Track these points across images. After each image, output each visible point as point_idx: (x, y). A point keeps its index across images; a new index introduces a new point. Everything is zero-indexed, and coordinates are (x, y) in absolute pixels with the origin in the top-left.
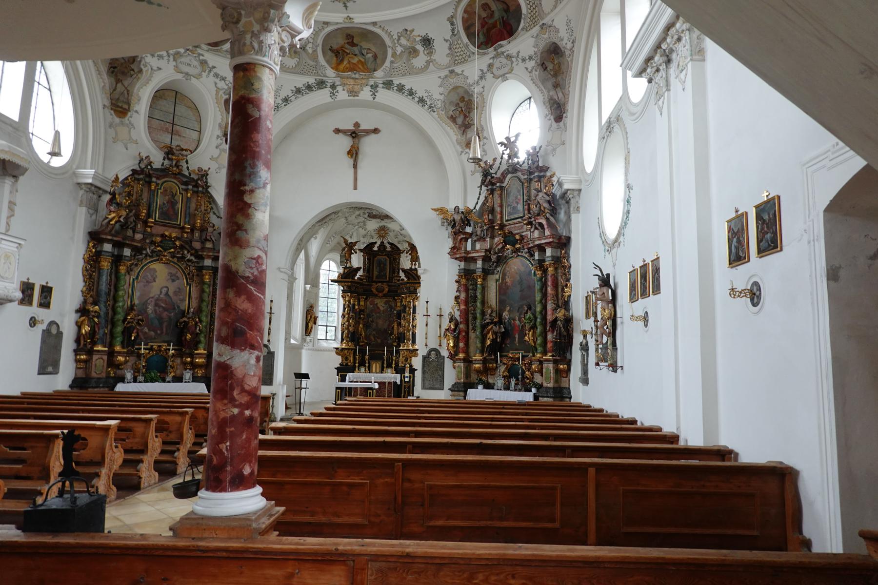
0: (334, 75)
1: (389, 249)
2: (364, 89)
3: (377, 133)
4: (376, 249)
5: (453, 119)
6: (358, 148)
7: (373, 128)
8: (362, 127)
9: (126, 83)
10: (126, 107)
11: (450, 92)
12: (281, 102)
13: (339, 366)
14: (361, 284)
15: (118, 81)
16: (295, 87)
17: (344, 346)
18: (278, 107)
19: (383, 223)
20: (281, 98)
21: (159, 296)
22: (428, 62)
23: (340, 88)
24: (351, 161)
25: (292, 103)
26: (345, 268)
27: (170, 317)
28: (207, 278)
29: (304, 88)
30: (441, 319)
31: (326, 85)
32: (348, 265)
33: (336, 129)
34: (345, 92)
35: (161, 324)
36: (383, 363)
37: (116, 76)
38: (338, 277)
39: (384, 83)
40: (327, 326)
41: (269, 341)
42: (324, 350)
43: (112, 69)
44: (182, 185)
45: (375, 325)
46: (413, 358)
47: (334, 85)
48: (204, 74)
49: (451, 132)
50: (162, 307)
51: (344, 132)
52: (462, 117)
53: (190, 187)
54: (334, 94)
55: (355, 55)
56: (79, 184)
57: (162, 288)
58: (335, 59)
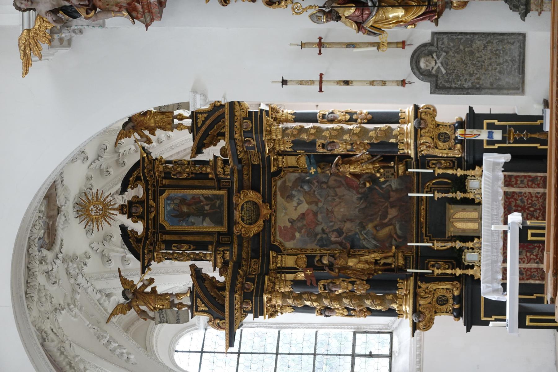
1: (139, 191)
4: (139, 227)
13: (461, 320)
14: (238, 265)
17: (408, 308)
19: (69, 209)
26: (194, 309)
30: (332, 44)
32: (187, 301)
36: (454, 201)
38: (219, 327)
40: (354, 356)
42: (420, 362)
45: (348, 225)
46: (439, 119)
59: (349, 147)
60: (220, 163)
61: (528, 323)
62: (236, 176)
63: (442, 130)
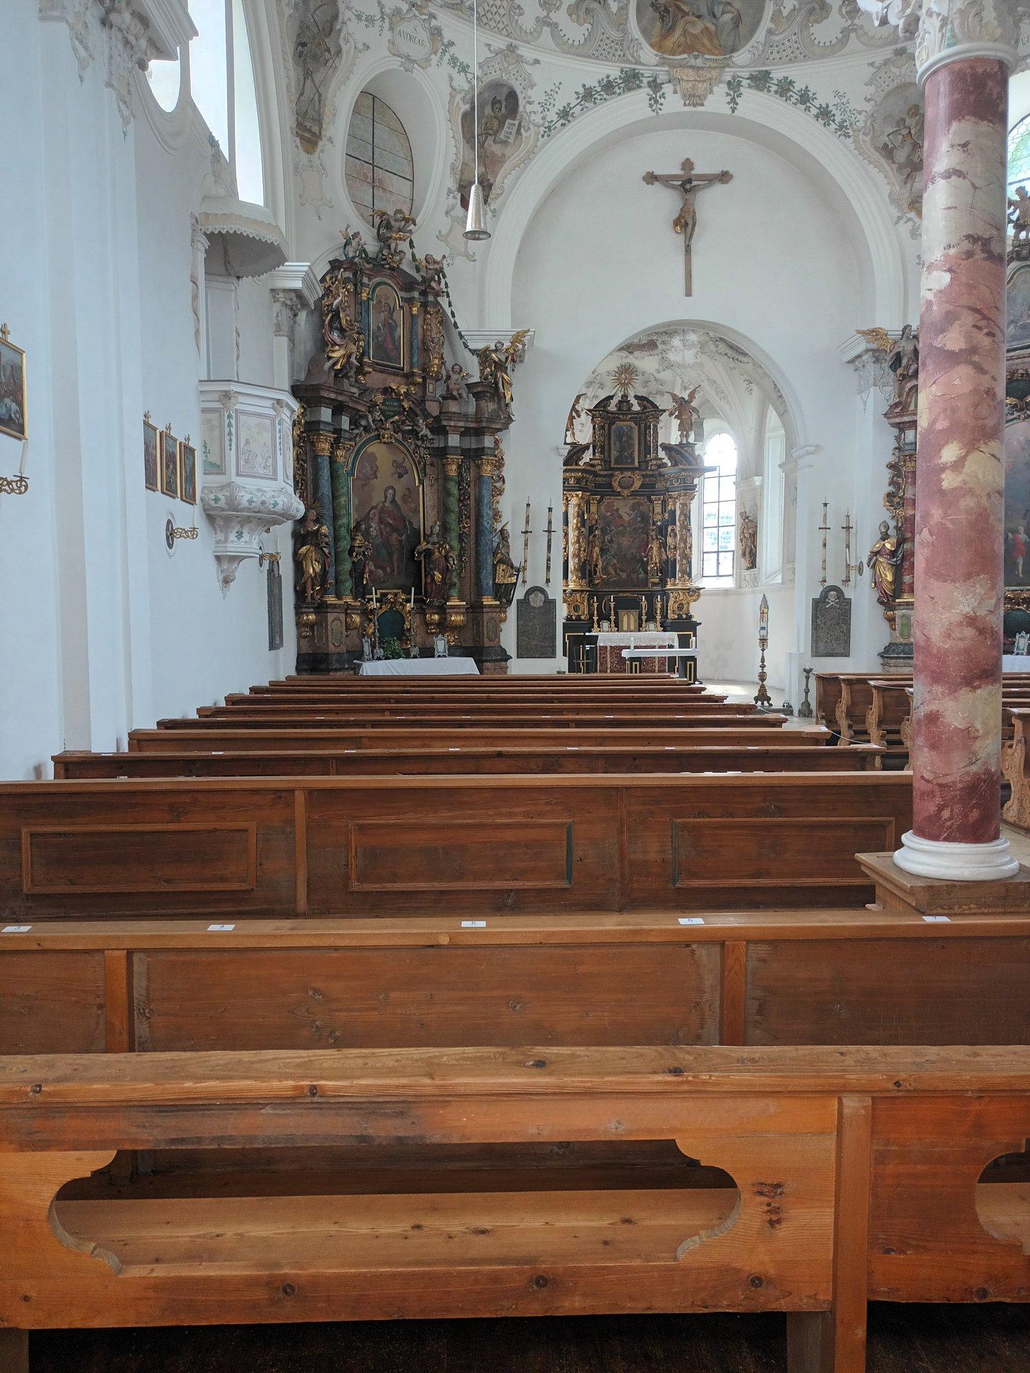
0: (655, 60)
1: (636, 408)
2: (715, 89)
3: (727, 182)
4: (612, 407)
5: (887, 152)
6: (694, 212)
7: (716, 170)
8: (698, 170)
9: (318, 77)
10: (315, 129)
11: (888, 95)
12: (555, 118)
14: (595, 474)
15: (308, 74)
16: (584, 86)
18: (549, 128)
20: (556, 110)
21: (384, 506)
22: (846, 32)
23: (667, 89)
24: (680, 239)
25: (822, 128)
27: (400, 541)
28: (453, 470)
29: (599, 89)
31: (641, 82)
33: (648, 173)
34: (678, 97)
35: (390, 554)
36: (640, 615)
37: (305, 62)
39: (751, 78)
41: (548, 581)
43: (300, 48)
44: (401, 290)
46: (692, 604)
47: (655, 81)
48: (435, 59)
49: (880, 178)
50: (390, 524)
51: (665, 180)
52: (907, 148)
53: (416, 294)
54: (656, 102)
55: (699, 17)
56: (273, 291)
57: (386, 490)
58: (658, 24)
59: (672, 547)
60: (659, 462)
61: (634, 663)
62: (650, 473)
63: (685, 606)
